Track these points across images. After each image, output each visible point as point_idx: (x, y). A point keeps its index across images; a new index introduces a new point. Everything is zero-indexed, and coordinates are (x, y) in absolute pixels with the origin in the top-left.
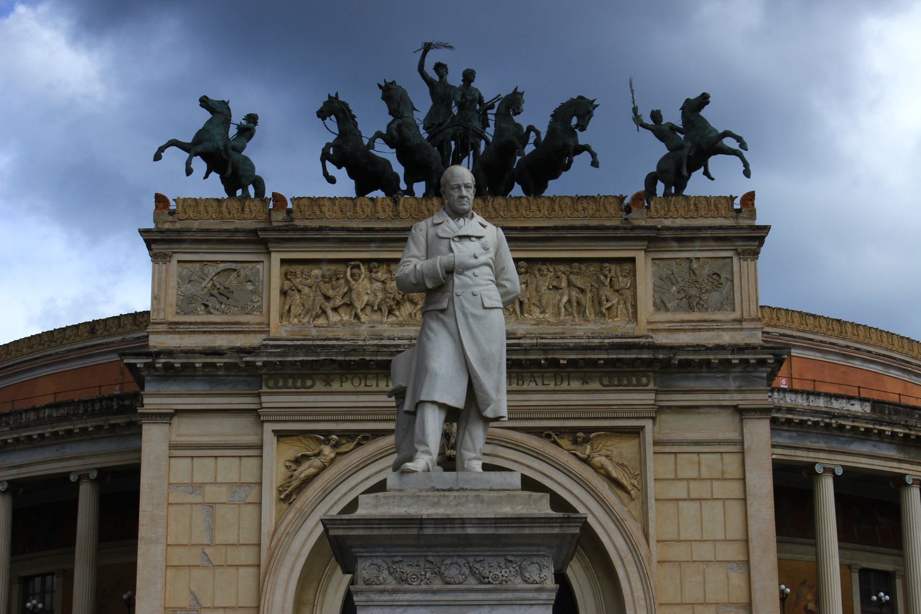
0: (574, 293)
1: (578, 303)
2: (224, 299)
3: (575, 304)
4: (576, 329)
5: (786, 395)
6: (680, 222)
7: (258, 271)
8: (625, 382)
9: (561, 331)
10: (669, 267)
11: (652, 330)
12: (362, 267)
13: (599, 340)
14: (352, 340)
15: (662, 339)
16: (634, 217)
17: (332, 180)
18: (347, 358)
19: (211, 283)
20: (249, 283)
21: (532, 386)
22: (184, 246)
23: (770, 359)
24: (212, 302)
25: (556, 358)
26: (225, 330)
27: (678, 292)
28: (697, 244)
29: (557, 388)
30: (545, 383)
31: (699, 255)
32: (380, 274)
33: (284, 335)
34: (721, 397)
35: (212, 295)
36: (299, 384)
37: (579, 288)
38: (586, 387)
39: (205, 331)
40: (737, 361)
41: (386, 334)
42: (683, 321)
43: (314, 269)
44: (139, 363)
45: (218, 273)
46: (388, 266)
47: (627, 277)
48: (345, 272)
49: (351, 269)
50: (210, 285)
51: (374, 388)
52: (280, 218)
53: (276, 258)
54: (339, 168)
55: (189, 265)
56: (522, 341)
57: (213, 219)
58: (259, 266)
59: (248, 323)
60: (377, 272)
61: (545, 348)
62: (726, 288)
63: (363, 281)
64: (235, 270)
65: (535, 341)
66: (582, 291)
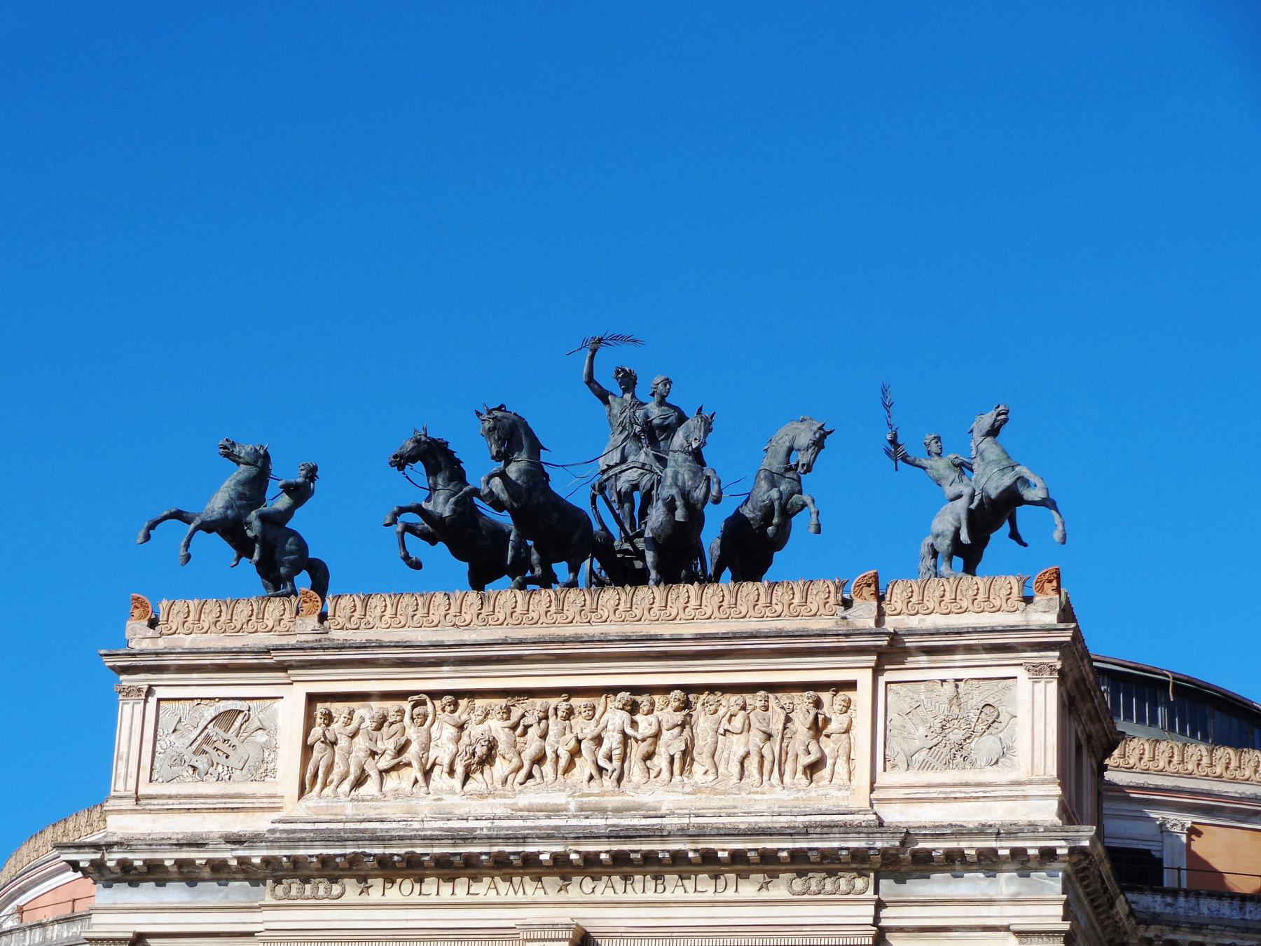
0: (757, 740)
5: (1201, 901)
6: (936, 621)
7: (275, 714)
8: (829, 887)
9: (731, 803)
11: (876, 799)
12: (429, 703)
13: (789, 818)
15: (894, 815)
17: (417, 565)
18: (388, 851)
20: (260, 732)
21: (679, 894)
23: (1061, 847)
24: (201, 762)
25: (713, 849)
26: (218, 806)
29: (719, 897)
30: (699, 888)
32: (457, 714)
34: (984, 911)
35: (204, 752)
36: (321, 892)
37: (764, 732)
38: (764, 895)
39: (189, 809)
40: (1007, 852)
41: (458, 812)
44: (82, 860)
47: (846, 712)
48: (401, 712)
49: (414, 707)
51: (433, 899)
52: (309, 629)
54: (433, 543)
55: (175, 704)
56: (665, 821)
59: (253, 796)
60: (453, 712)
61: (700, 834)
64: (241, 711)
65: (686, 821)
66: (769, 736)
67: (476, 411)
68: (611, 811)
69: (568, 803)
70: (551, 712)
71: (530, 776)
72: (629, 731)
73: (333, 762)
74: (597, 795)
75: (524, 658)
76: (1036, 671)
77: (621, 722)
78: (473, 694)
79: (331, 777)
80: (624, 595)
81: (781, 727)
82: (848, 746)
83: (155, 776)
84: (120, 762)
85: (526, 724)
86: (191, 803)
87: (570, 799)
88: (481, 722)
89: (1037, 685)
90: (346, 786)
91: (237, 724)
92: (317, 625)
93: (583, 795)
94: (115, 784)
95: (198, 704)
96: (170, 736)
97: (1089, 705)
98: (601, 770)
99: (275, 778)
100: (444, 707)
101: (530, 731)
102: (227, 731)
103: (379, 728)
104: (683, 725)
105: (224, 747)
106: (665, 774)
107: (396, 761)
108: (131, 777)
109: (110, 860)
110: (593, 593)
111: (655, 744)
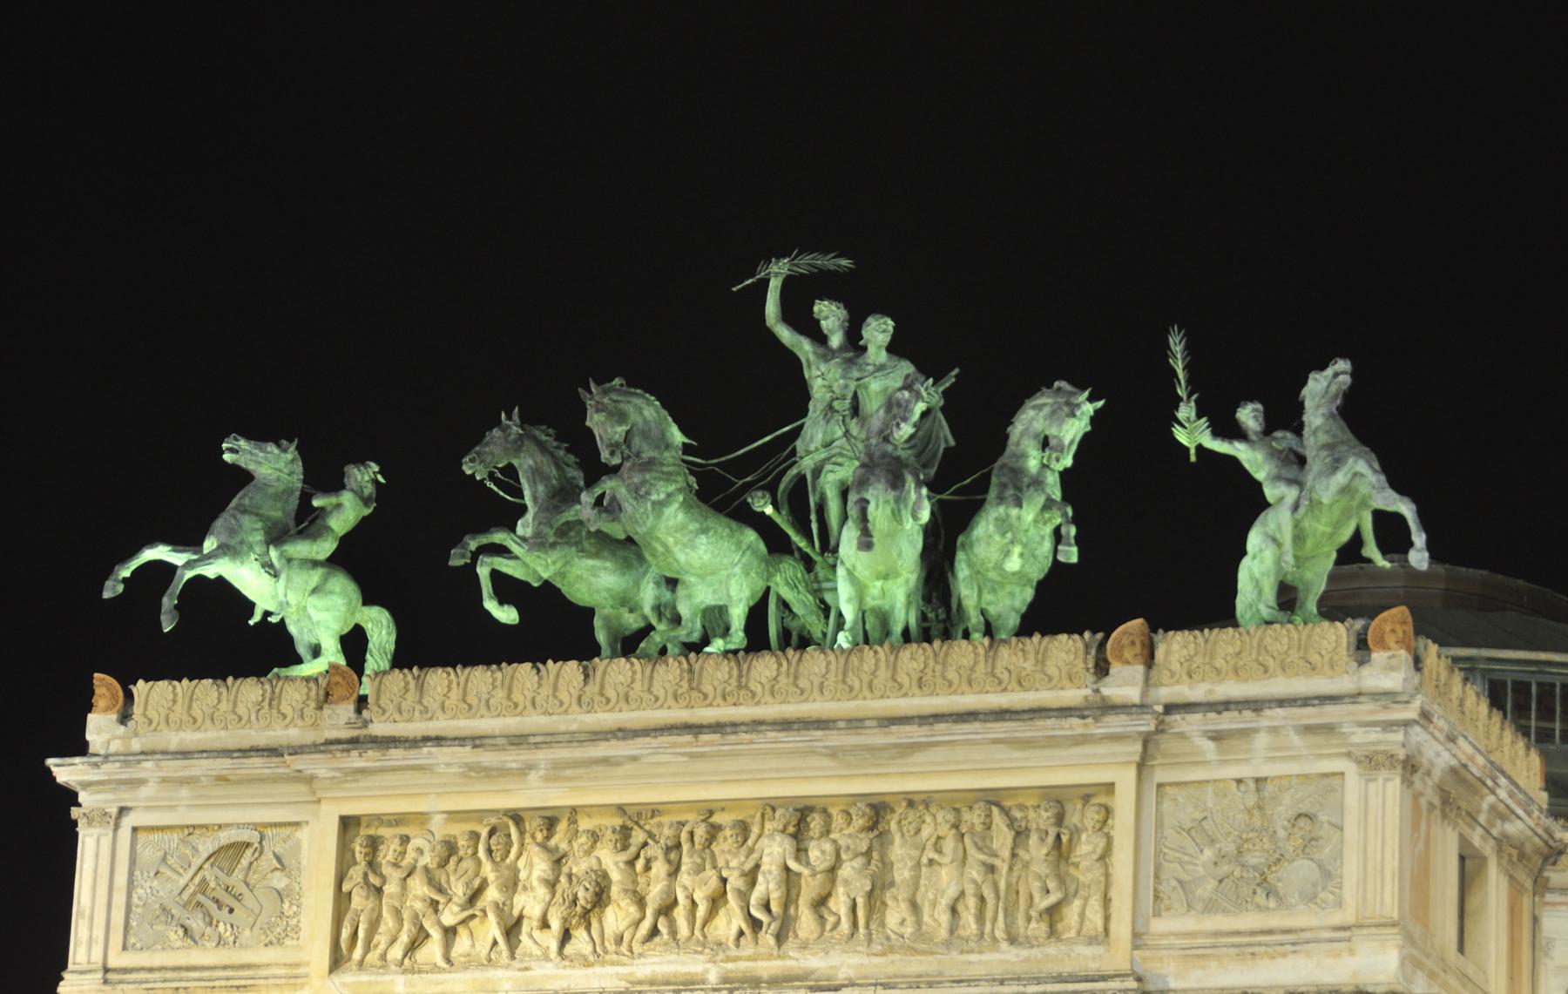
1: (982, 899)
3: (971, 902)
4: (970, 963)
7: (298, 843)
22: (145, 792)
24: (197, 923)
26: (217, 983)
27: (1216, 863)
28: (1262, 741)
31: (1265, 770)
42: (1217, 934)
43: (415, 837)
46: (573, 821)
49: (492, 833)
50: (197, 880)
55: (156, 836)
58: (303, 835)
59: (268, 965)
60: (548, 838)
62: (1326, 853)
63: (518, 858)
64: (248, 845)
66: (991, 869)
68: (767, 982)
69: (707, 971)
70: (684, 836)
71: (654, 932)
72: (793, 865)
73: (380, 915)
74: (749, 959)
76: (1371, 762)
77: (780, 850)
78: (574, 810)
79: (377, 938)
80: (785, 663)
81: (1006, 854)
82: (1102, 879)
83: (132, 940)
84: (81, 921)
85: (649, 855)
86: (181, 980)
87: (710, 965)
88: (588, 853)
89: (1372, 786)
90: (396, 952)
91: (244, 862)
92: (353, 715)
93: (729, 959)
94: (75, 953)
96: (152, 882)
97: (1491, 799)
98: (756, 924)
99: (298, 939)
102: (230, 873)
103: (443, 864)
104: (868, 854)
105: (227, 900)
106: (845, 925)
107: (466, 913)
108: (97, 943)
110: (741, 662)
111: (833, 881)
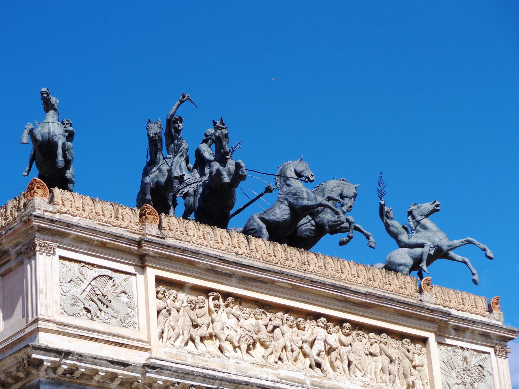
2: (103, 308)
10: (448, 353)
14: (227, 373)
16: (426, 299)
19: (90, 286)
22: (66, 241)
28: (468, 334)
33: (164, 357)
35: (91, 299)
45: (95, 279)
49: (213, 299)
53: (152, 273)
57: (90, 219)
58: (133, 278)
64: (111, 278)
67: (213, 120)
69: (305, 379)
75: (276, 284)
95: (84, 266)
100: (229, 304)
101: (277, 330)
109: (65, 364)
